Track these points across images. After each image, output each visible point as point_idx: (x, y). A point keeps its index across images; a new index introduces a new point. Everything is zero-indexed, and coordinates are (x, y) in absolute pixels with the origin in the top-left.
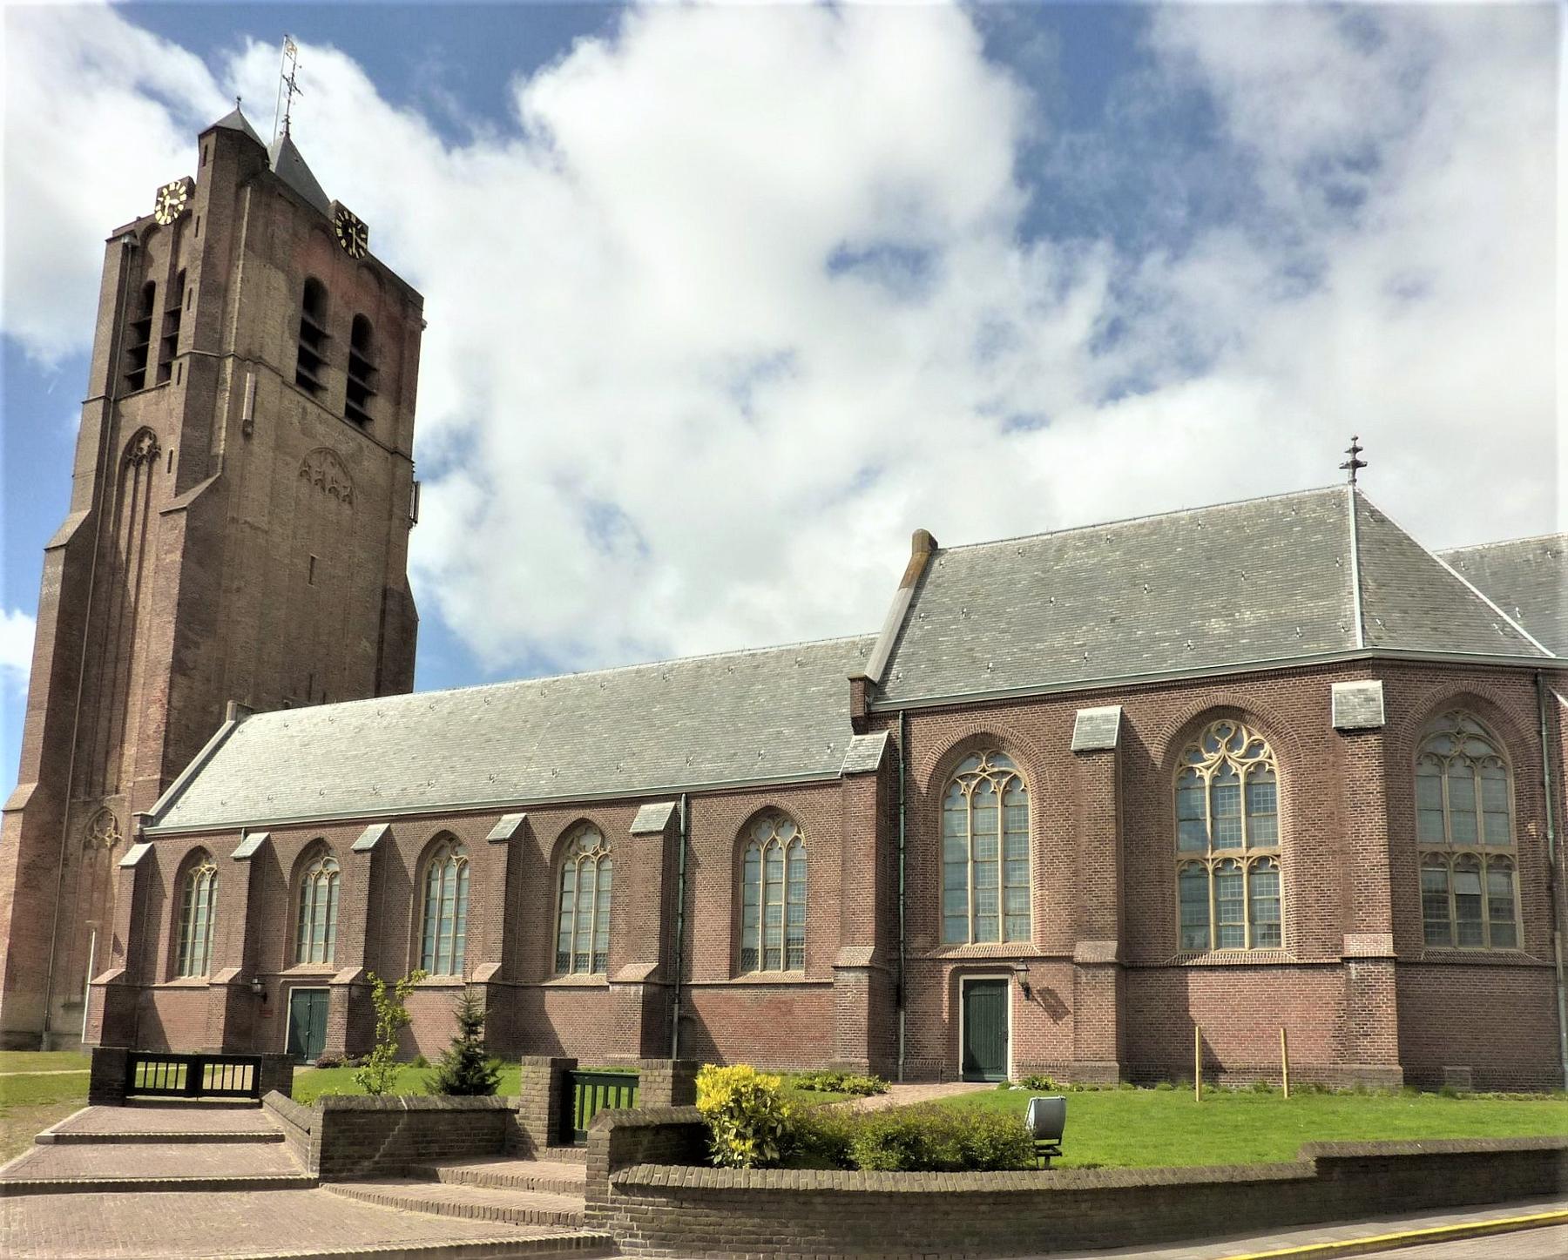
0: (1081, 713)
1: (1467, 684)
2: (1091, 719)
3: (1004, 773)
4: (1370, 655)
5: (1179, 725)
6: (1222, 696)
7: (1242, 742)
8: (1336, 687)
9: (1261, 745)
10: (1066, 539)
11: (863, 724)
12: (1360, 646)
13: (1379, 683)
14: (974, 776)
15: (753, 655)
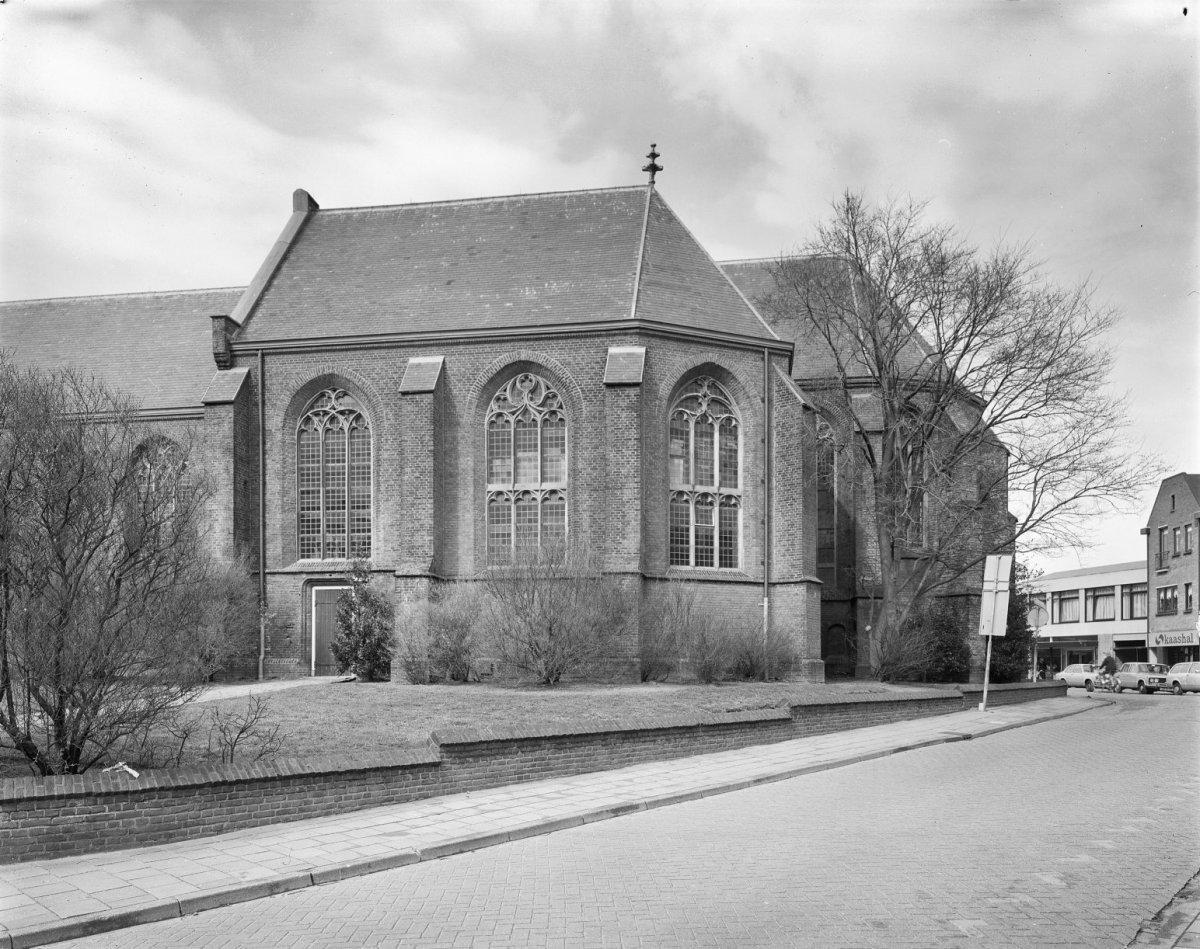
0: (413, 360)
1: (712, 356)
2: (419, 365)
3: (351, 412)
4: (636, 324)
5: (490, 375)
6: (525, 354)
7: (541, 394)
8: (613, 350)
9: (555, 396)
10: (425, 210)
11: (226, 361)
12: (632, 317)
13: (642, 350)
14: (326, 413)
15: (157, 298)
